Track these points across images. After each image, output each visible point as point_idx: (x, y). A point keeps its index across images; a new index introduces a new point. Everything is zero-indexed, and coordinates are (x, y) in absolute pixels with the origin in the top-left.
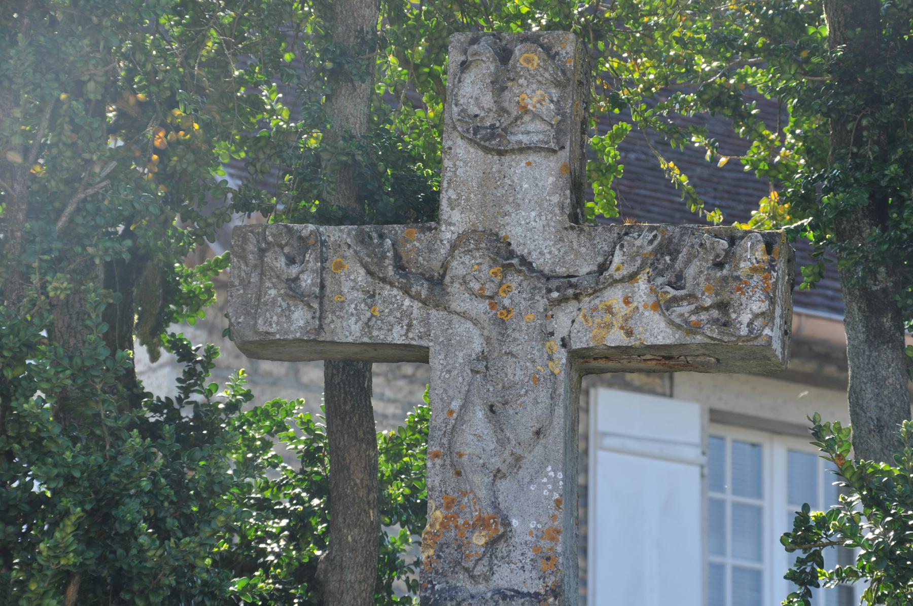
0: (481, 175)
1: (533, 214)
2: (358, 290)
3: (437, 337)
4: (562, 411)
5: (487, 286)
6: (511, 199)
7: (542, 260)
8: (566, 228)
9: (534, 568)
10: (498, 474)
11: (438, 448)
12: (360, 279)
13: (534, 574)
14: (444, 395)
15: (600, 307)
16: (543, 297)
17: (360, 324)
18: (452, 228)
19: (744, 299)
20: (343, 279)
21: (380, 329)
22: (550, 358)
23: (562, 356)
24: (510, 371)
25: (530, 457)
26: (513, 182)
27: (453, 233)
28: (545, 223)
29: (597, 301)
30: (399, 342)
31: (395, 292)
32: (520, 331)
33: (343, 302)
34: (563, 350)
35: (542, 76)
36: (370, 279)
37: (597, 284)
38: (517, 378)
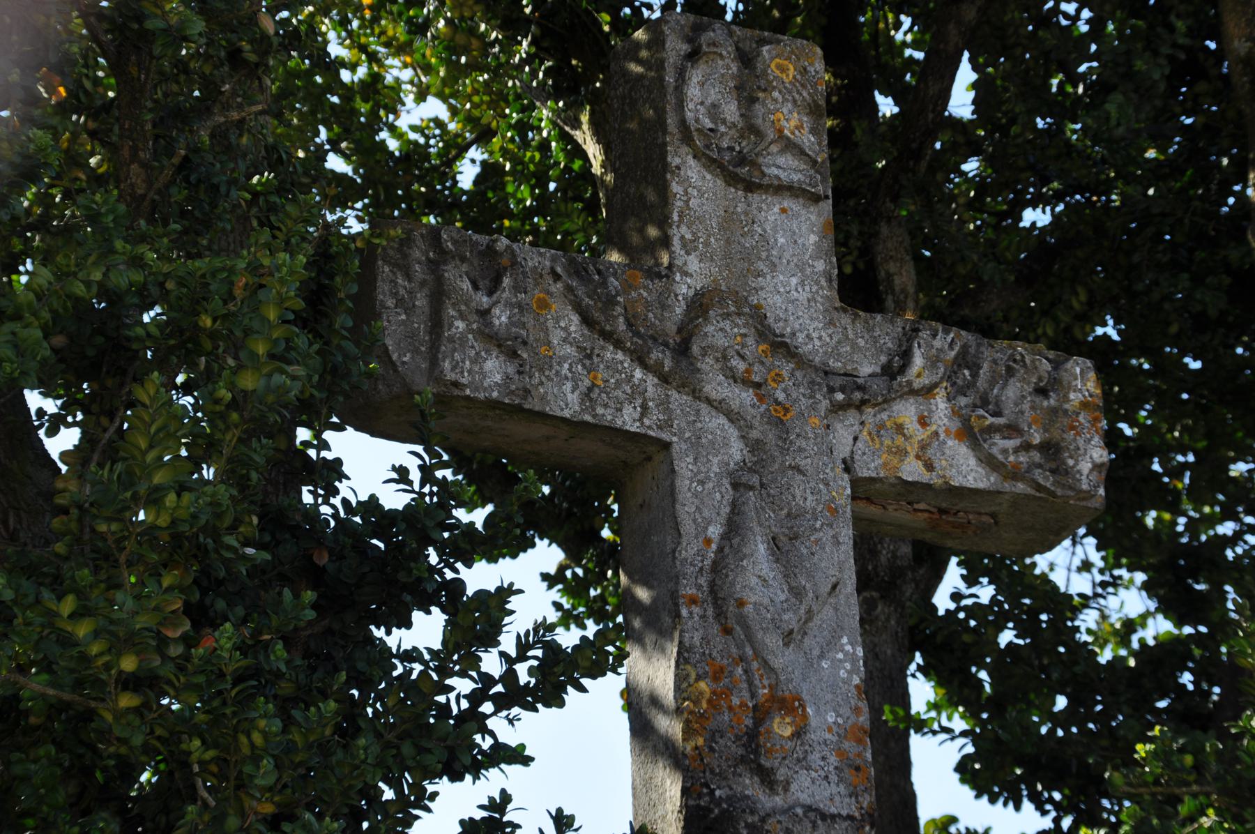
0: (722, 213)
1: (794, 281)
2: (571, 344)
6: (764, 255)
8: (836, 309)
9: (841, 780)
11: (694, 591)
13: (842, 788)
15: (888, 424)
17: (577, 393)
20: (550, 324)
24: (798, 493)
26: (765, 231)
27: (689, 287)
29: (884, 416)
30: (632, 429)
31: (620, 356)
32: (807, 438)
33: (551, 357)
35: (798, 92)
38: (808, 503)
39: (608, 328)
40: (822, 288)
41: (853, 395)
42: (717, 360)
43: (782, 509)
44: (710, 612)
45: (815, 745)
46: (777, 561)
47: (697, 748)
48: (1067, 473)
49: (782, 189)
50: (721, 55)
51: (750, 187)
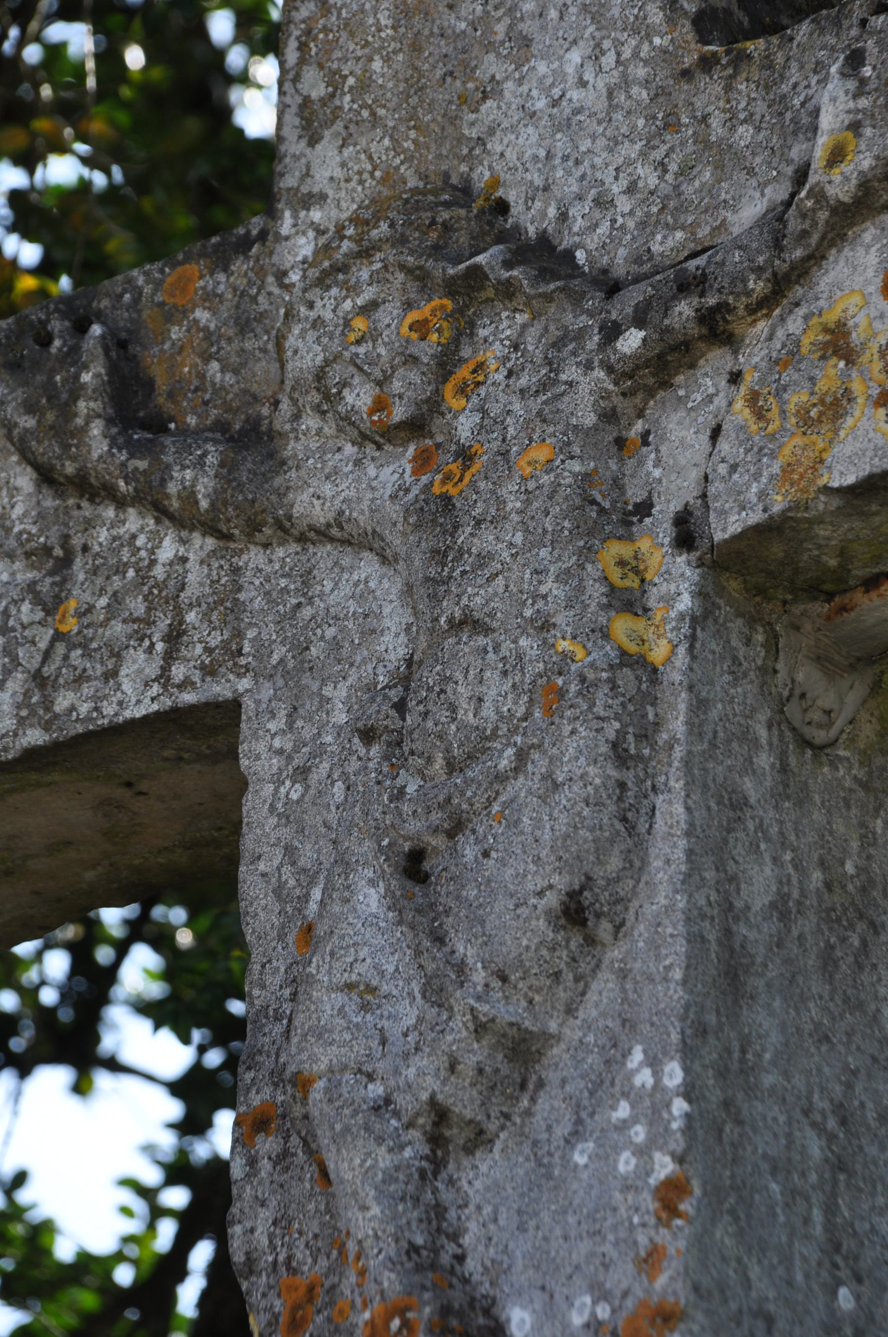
1: (575, 56)
3: (262, 649)
4: (679, 809)
5: (397, 386)
6: (500, 29)
7: (604, 229)
8: (686, 74)
10: (444, 1136)
12: (18, 511)
15: (806, 341)
16: (588, 366)
21: (81, 679)
22: (629, 601)
23: (677, 584)
25: (572, 1033)
28: (614, 78)
29: (794, 325)
30: (139, 712)
31: (133, 520)
34: (681, 559)
36: (49, 503)
37: (777, 245)
38: (488, 710)
39: (70, 468)
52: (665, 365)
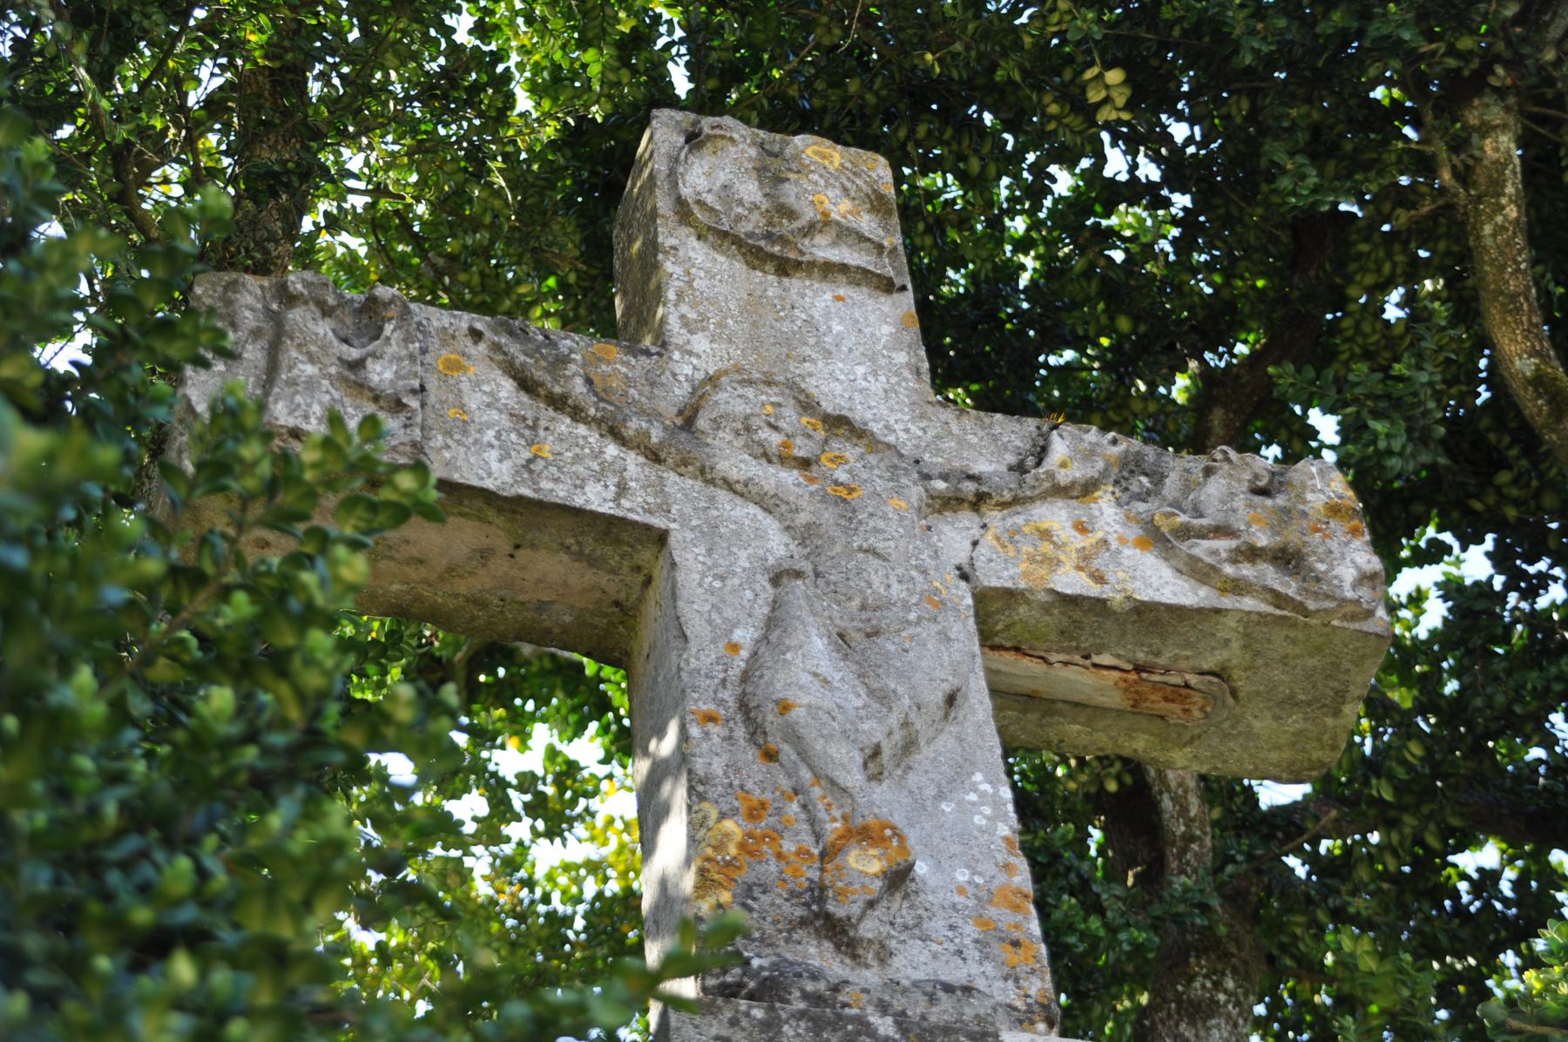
0: (745, 297)
1: (860, 370)
2: (500, 411)
5: (799, 441)
6: (812, 341)
11: (712, 707)
14: (714, 616)
15: (1026, 530)
18: (695, 361)
19: (1333, 545)
20: (465, 386)
27: (695, 368)
29: (1019, 520)
30: (601, 510)
31: (582, 430)
32: (885, 517)
39: (557, 390)
40: (905, 379)
41: (966, 497)
42: (737, 433)
43: (850, 599)
44: (740, 732)
45: (935, 909)
46: (846, 657)
47: (720, 906)
48: (1318, 580)
49: (829, 270)
50: (731, 139)
51: (785, 268)
52: (948, 504)
